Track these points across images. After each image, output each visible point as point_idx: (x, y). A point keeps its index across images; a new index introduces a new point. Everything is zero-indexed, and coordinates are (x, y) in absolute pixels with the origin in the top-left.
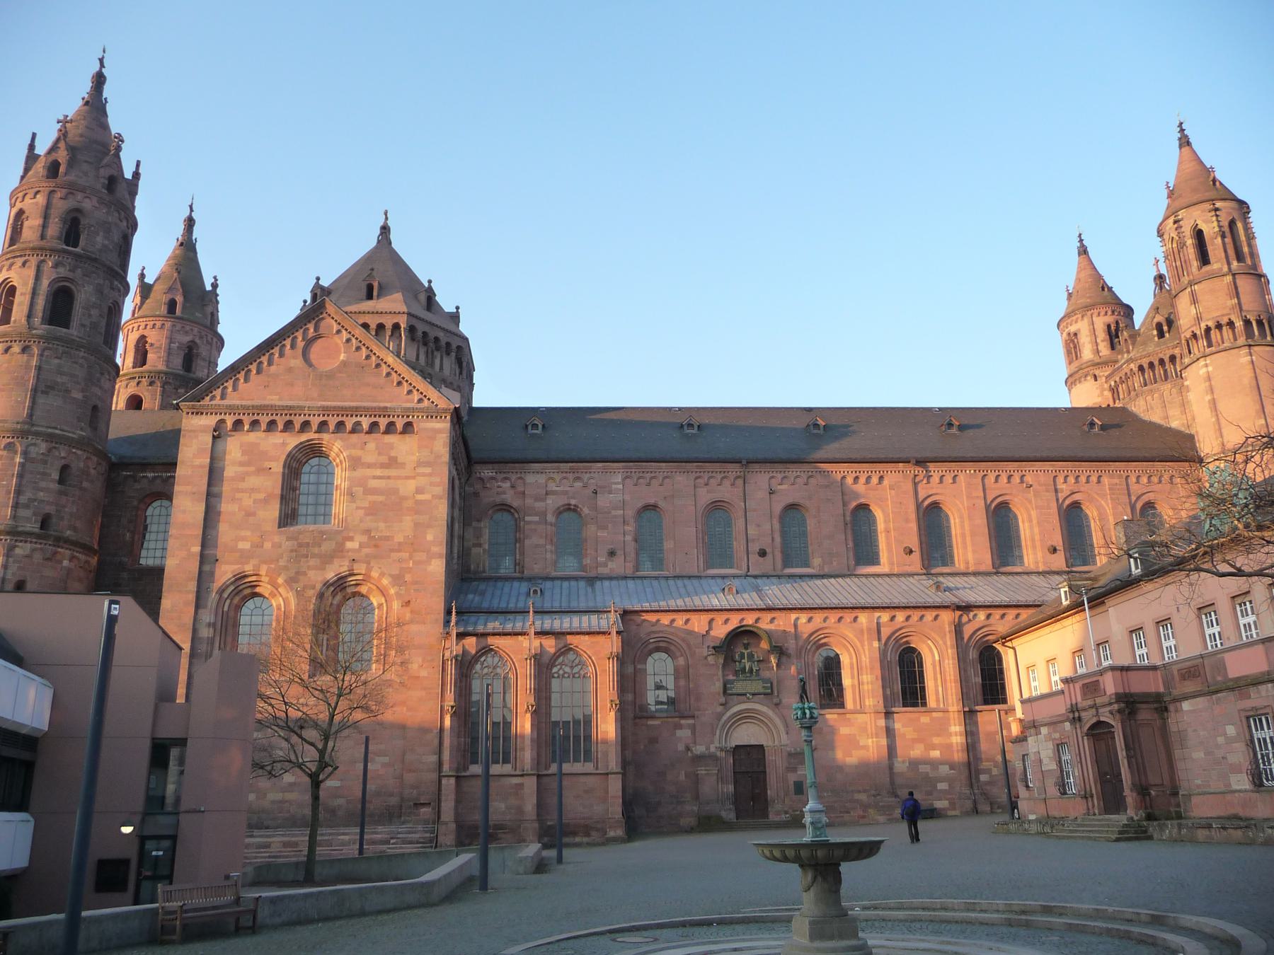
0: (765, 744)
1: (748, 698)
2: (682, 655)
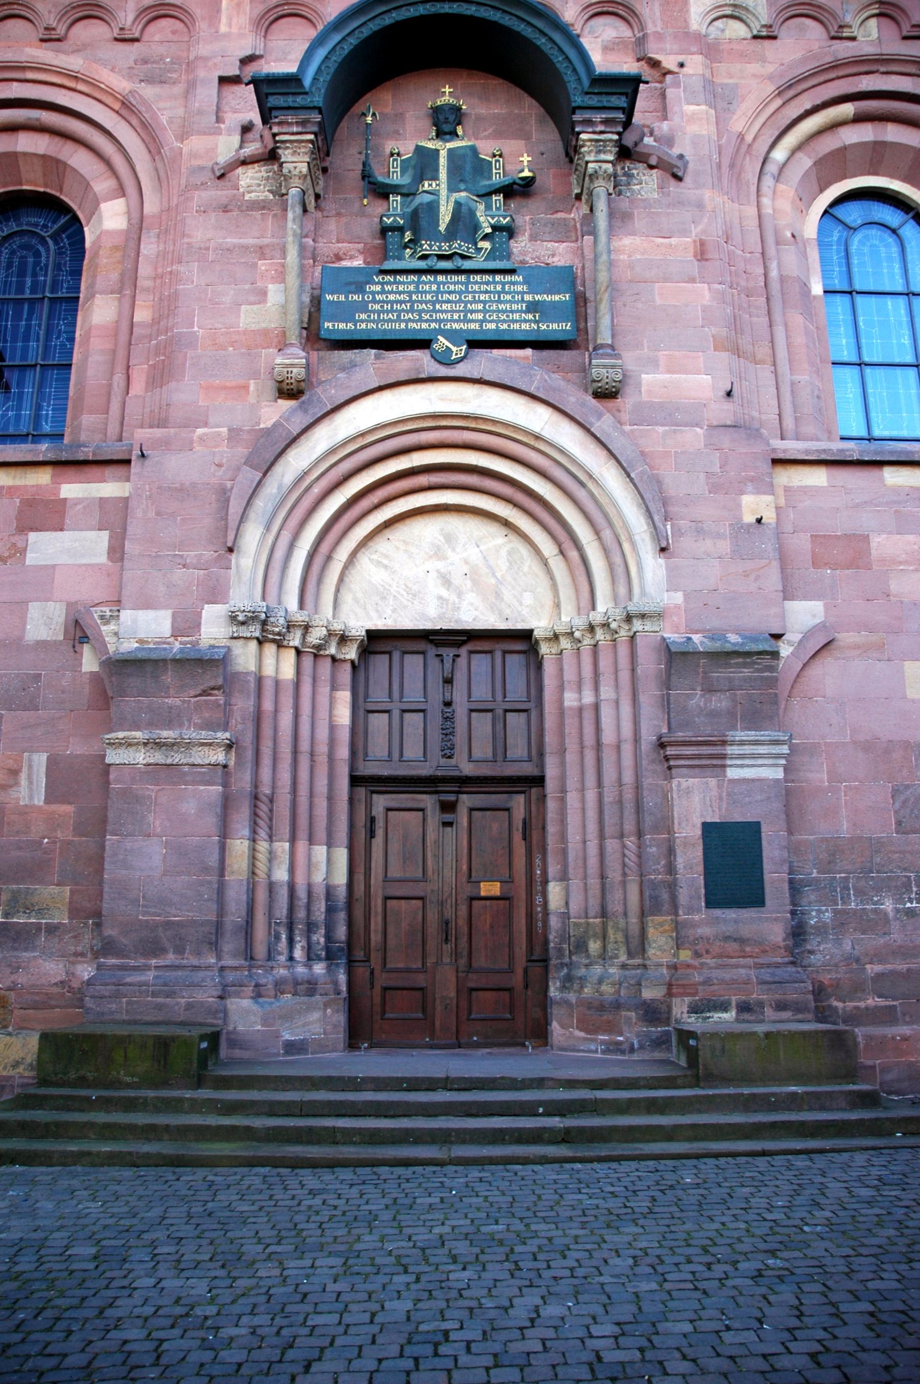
0: (540, 624)
1: (444, 359)
2: (121, 192)
